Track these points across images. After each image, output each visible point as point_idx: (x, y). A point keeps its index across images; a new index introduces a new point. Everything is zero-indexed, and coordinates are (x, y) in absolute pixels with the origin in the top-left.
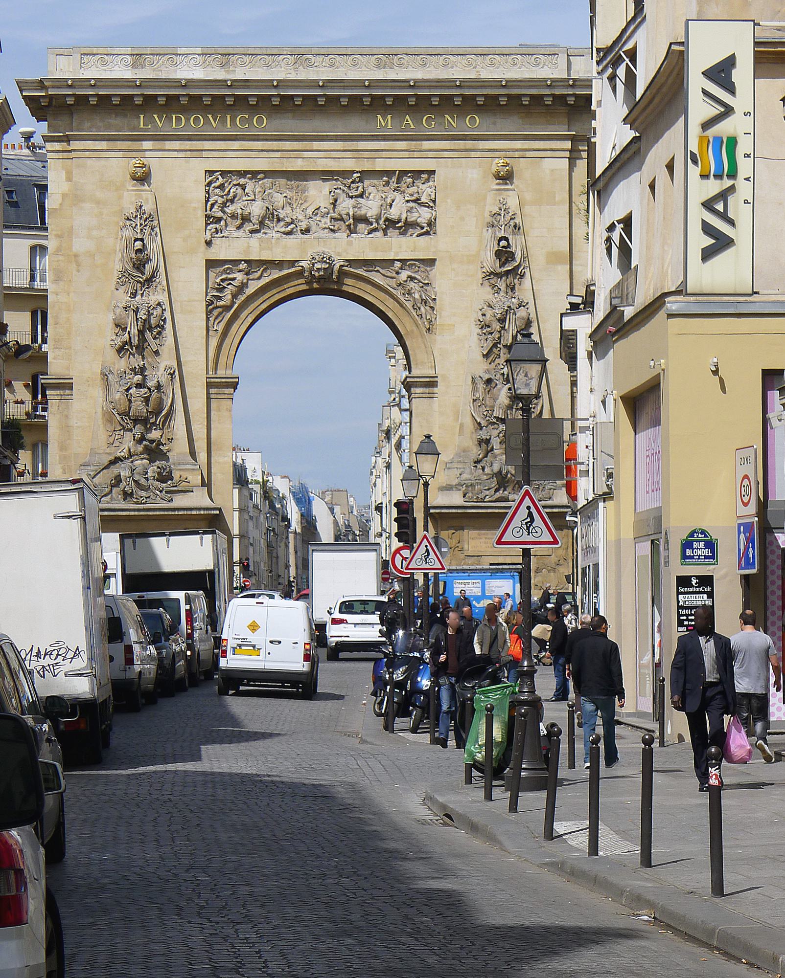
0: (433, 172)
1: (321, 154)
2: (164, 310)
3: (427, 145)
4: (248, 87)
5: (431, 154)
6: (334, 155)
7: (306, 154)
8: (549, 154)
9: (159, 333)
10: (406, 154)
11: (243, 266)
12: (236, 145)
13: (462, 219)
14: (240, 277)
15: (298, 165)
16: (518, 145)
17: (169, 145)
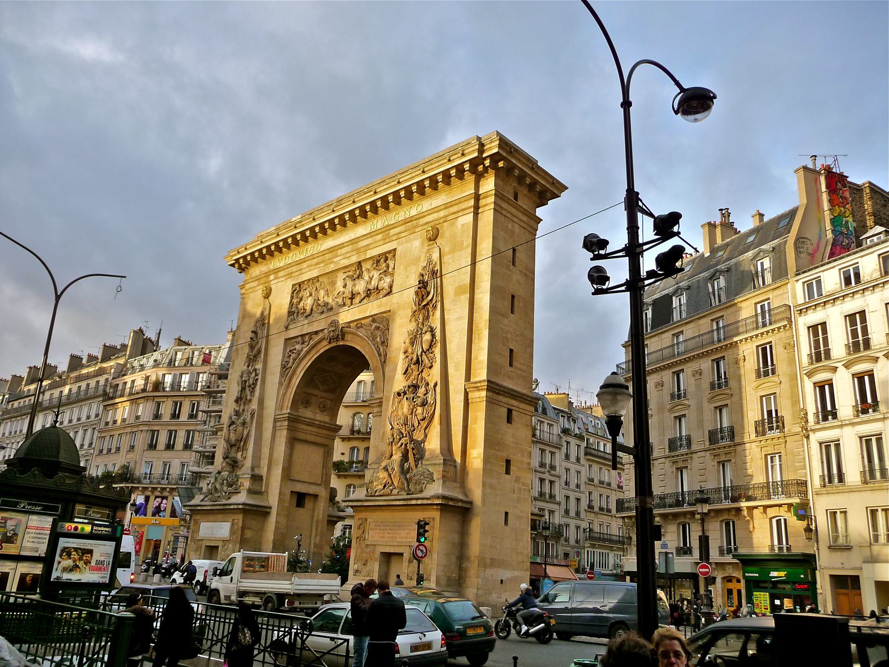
0: (395, 250)
1: (341, 257)
2: (256, 375)
3: (392, 232)
4: (303, 225)
5: (394, 238)
6: (348, 255)
7: (336, 260)
8: (461, 214)
9: (253, 388)
10: (382, 242)
11: (300, 339)
12: (305, 265)
13: (407, 277)
14: (298, 347)
15: (332, 267)
16: (442, 214)
17: (282, 274)
